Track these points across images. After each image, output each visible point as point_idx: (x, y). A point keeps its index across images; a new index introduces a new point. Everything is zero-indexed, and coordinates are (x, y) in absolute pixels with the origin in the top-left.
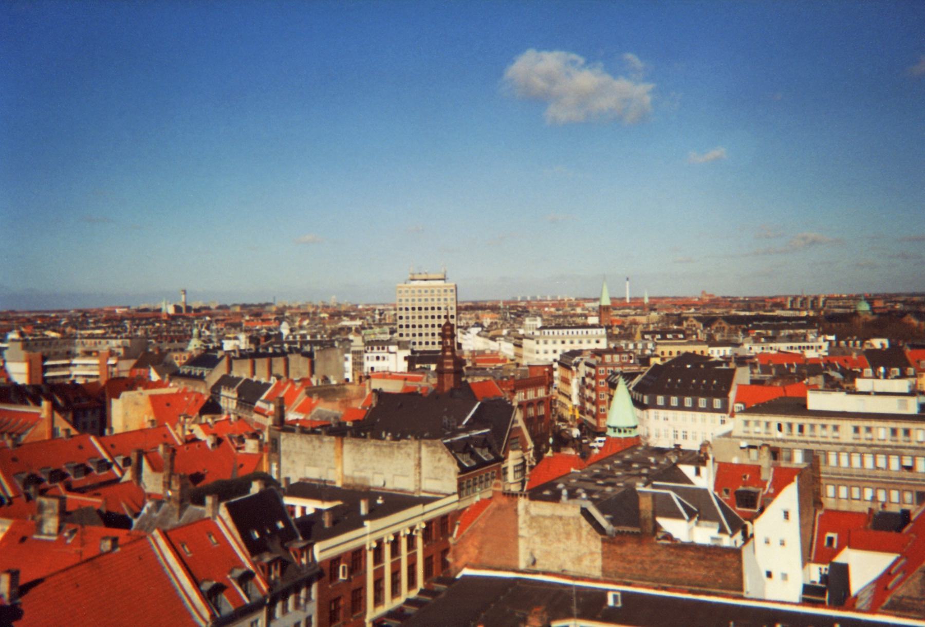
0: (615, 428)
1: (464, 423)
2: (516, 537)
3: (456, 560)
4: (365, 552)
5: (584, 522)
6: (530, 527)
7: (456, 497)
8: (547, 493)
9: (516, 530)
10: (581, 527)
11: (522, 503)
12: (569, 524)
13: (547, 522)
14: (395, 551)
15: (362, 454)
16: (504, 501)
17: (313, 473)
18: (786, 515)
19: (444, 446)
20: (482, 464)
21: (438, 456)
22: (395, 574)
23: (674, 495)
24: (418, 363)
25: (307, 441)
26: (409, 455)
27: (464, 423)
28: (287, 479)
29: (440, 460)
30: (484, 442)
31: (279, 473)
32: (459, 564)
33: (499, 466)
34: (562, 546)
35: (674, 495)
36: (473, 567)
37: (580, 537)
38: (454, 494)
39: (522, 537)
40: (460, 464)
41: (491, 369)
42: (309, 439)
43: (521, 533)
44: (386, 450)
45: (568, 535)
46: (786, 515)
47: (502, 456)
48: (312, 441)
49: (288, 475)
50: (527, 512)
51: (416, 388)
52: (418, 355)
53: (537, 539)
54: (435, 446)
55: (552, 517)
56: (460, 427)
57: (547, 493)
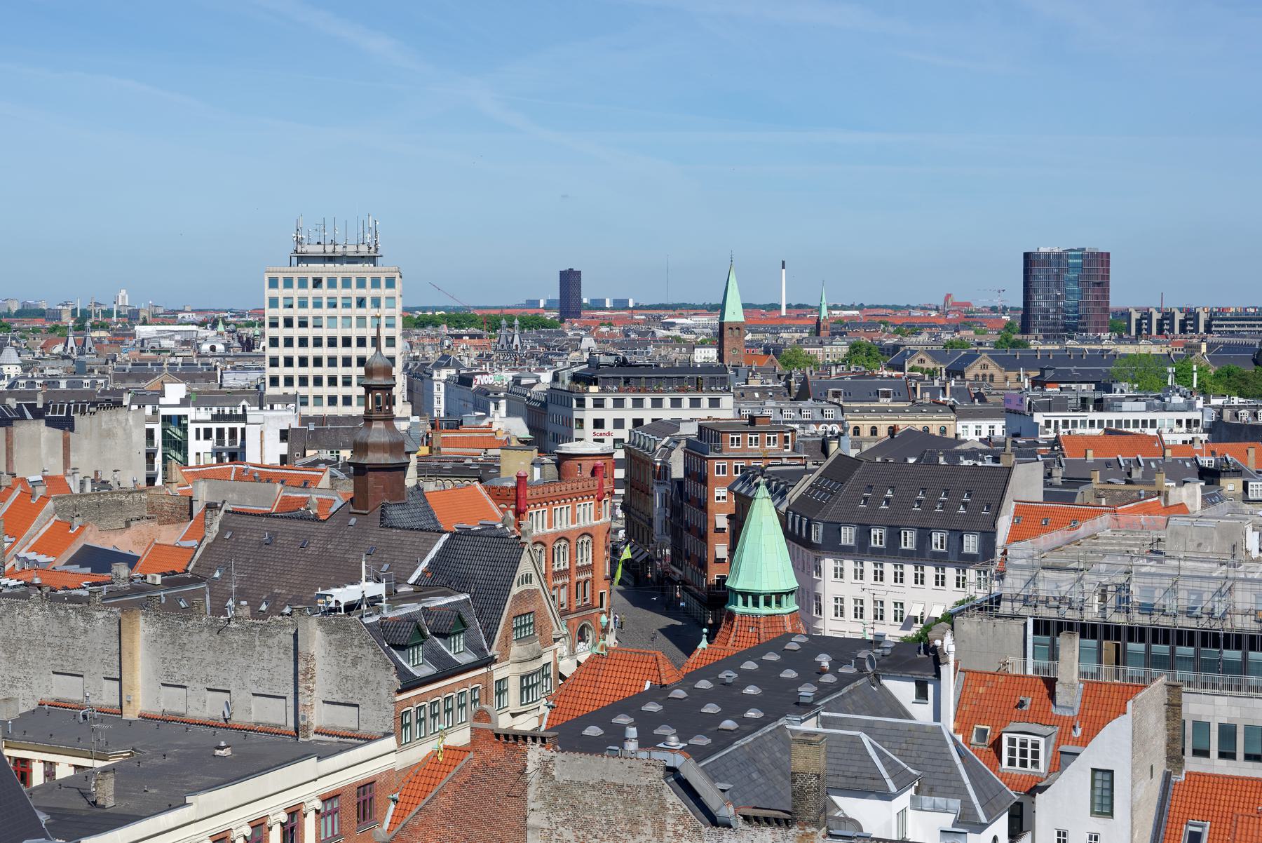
0: (745, 594)
1: (412, 580)
5: (672, 798)
6: (552, 806)
8: (593, 731)
10: (664, 808)
12: (636, 802)
13: (590, 797)
15: (182, 647)
16: (496, 753)
19: (366, 632)
20: (449, 670)
21: (352, 652)
23: (865, 739)
25: (57, 617)
27: (412, 580)
29: (354, 664)
30: (452, 625)
33: (488, 676)
35: (865, 739)
37: (660, 830)
38: (387, 735)
39: (535, 828)
40: (402, 672)
42: (62, 613)
43: (532, 820)
47: (494, 652)
48: (68, 618)
52: (312, 428)
54: (346, 629)
55: (600, 786)
56: (403, 589)
57: (593, 731)
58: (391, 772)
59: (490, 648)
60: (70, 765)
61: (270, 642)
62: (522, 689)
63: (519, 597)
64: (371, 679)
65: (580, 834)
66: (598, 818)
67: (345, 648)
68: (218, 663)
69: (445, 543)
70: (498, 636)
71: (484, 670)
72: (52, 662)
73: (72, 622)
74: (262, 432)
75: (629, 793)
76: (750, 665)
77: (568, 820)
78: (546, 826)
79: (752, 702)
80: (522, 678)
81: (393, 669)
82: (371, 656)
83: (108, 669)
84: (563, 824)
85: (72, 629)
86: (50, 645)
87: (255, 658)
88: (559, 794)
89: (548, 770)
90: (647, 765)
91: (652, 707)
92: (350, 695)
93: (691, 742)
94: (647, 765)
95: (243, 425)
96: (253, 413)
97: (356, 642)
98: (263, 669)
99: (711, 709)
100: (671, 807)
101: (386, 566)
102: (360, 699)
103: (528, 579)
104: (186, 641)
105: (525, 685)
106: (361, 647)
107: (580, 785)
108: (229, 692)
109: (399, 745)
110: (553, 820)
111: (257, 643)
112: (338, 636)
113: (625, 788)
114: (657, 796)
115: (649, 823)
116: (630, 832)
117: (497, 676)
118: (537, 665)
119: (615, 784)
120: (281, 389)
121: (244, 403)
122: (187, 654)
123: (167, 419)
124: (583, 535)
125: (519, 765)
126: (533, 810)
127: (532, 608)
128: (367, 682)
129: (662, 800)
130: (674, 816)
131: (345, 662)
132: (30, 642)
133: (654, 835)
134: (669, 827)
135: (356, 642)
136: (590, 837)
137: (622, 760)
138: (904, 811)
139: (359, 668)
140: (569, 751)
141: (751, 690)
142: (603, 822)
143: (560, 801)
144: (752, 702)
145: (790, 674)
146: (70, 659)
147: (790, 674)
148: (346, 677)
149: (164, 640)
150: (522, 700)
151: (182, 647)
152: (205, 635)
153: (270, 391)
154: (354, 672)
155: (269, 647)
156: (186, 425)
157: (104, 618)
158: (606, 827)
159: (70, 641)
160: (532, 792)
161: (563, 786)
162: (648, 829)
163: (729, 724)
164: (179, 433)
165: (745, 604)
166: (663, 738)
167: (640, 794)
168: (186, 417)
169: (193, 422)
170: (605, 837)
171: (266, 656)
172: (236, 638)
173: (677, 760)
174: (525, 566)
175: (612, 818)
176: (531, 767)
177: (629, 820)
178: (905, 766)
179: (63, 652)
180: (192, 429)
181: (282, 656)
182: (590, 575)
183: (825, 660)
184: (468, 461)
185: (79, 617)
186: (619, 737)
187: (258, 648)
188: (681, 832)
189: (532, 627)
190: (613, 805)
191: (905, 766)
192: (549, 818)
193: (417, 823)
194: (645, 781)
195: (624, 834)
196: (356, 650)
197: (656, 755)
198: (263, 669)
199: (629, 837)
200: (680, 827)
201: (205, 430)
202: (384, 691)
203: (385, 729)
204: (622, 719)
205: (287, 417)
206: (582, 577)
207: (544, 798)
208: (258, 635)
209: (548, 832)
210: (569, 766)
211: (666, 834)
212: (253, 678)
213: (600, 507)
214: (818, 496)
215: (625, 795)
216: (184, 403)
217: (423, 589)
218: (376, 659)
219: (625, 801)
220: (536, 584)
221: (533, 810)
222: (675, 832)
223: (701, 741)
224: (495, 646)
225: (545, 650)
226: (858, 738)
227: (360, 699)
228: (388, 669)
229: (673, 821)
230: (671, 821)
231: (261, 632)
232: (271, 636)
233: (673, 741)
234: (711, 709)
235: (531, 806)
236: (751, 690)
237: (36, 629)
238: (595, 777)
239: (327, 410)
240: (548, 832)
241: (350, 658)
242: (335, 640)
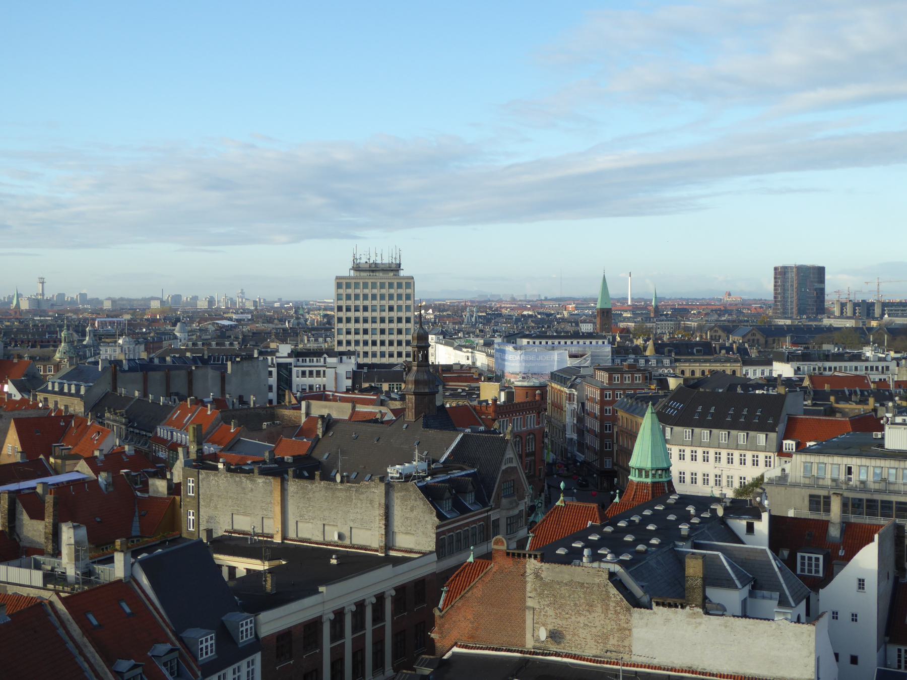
2: (524, 608)
3: (443, 637)
4: (322, 623)
5: (613, 591)
6: (541, 595)
7: (434, 556)
8: (561, 551)
9: (523, 600)
10: (608, 597)
11: (532, 564)
13: (564, 591)
14: (358, 625)
15: (309, 499)
17: (244, 523)
18: (861, 583)
22: (358, 654)
24: (365, 381)
25: (235, 481)
26: (371, 502)
28: (209, 532)
29: (412, 510)
31: (197, 523)
32: (447, 643)
33: (488, 517)
34: (582, 619)
36: (460, 646)
37: (606, 609)
39: (529, 608)
41: (463, 390)
42: (238, 479)
43: (530, 603)
44: (342, 495)
45: (591, 606)
46: (861, 583)
49: (210, 526)
50: (537, 575)
51: (375, 413)
53: (550, 612)
54: (407, 490)
55: (570, 583)
57: (561, 551)
58: (434, 574)
59: (489, 501)
60: (244, 568)
61: (361, 497)
62: (507, 525)
63: (506, 472)
64: (421, 519)
65: (557, 612)
66: (568, 603)
67: (406, 500)
68: (330, 509)
69: (461, 439)
70: (494, 494)
71: (486, 514)
72: (232, 508)
73: (244, 485)
74: (336, 373)
75: (588, 588)
76: (647, 512)
77: (551, 603)
78: (537, 606)
79: (653, 534)
80: (507, 518)
81: (435, 513)
82: (422, 506)
83: (265, 512)
84: (548, 606)
85: (244, 489)
86: (231, 497)
87: (352, 506)
88: (545, 587)
89: (539, 574)
90: (598, 571)
91: (594, 537)
92: (409, 528)
93: (621, 558)
94: (598, 571)
95: (324, 369)
96: (332, 361)
97: (413, 497)
98: (357, 512)
99: (629, 538)
100: (613, 596)
101: (426, 452)
102: (415, 531)
103: (511, 460)
104: (311, 496)
105: (509, 523)
106: (416, 501)
107: (558, 583)
108: (337, 526)
109: (438, 558)
110: (542, 603)
111: (354, 497)
112: (403, 494)
113: (585, 584)
114: (604, 589)
115: (599, 605)
116: (588, 611)
117: (492, 519)
118: (516, 512)
119: (579, 583)
120: (343, 348)
121: (325, 356)
122: (312, 504)
123: (279, 365)
124: (529, 435)
125: (522, 571)
126: (530, 597)
127: (512, 478)
128: (420, 521)
129: (607, 592)
130: (614, 602)
131: (406, 509)
132: (219, 496)
133: (602, 613)
134: (611, 608)
135: (413, 497)
136: (564, 613)
137: (583, 568)
138: (745, 599)
139: (415, 513)
140: (552, 563)
141: (651, 527)
142: (572, 605)
143: (546, 592)
144: (653, 534)
145: (672, 517)
146: (242, 506)
147: (672, 517)
148: (407, 518)
149: (298, 495)
150: (507, 532)
151: (309, 499)
152: (323, 493)
153: (337, 349)
154: (412, 515)
155: (361, 500)
156: (291, 369)
157: (263, 482)
158: (574, 608)
159: (243, 495)
160: (529, 587)
161: (548, 584)
162: (599, 609)
163: (641, 547)
164: (287, 373)
165: (640, 475)
166: (605, 556)
167: (594, 589)
168: (291, 364)
169: (295, 366)
170: (573, 613)
171: (359, 505)
172: (341, 494)
173: (617, 568)
174: (510, 454)
175: (578, 602)
176: (528, 571)
177: (588, 604)
178: (746, 572)
179: (238, 502)
180: (294, 370)
181: (369, 505)
182: (533, 458)
183: (691, 509)
184: (460, 390)
185: (248, 482)
186: (579, 554)
187: (354, 501)
188: (619, 611)
189: (512, 488)
190: (578, 595)
191: (746, 572)
192: (539, 602)
193: (460, 605)
194: (597, 580)
195: (585, 612)
196: (413, 502)
197: (603, 565)
198: (357, 512)
199: (588, 614)
200: (619, 608)
201: (317, 371)
202: (429, 526)
203: (430, 549)
204: (578, 545)
205: (350, 364)
206: (529, 459)
207: (536, 590)
208: (354, 493)
209: (539, 610)
210: (548, 571)
211: (609, 612)
212: (351, 518)
213: (539, 417)
214: (669, 412)
215: (585, 589)
216: (290, 356)
217: (447, 466)
218: (424, 507)
219: (585, 593)
220: (514, 465)
221: (530, 597)
222: (616, 611)
223: (626, 557)
224: (492, 500)
225: (520, 502)
226: (718, 556)
227: (415, 531)
228: (432, 513)
229: (614, 605)
230: (612, 604)
231: (356, 491)
232: (362, 493)
233: (609, 557)
234: (629, 538)
235: (529, 595)
236: (651, 527)
237: (222, 488)
238: (566, 578)
239: (376, 361)
240: (539, 610)
241: (409, 507)
242: (400, 496)
